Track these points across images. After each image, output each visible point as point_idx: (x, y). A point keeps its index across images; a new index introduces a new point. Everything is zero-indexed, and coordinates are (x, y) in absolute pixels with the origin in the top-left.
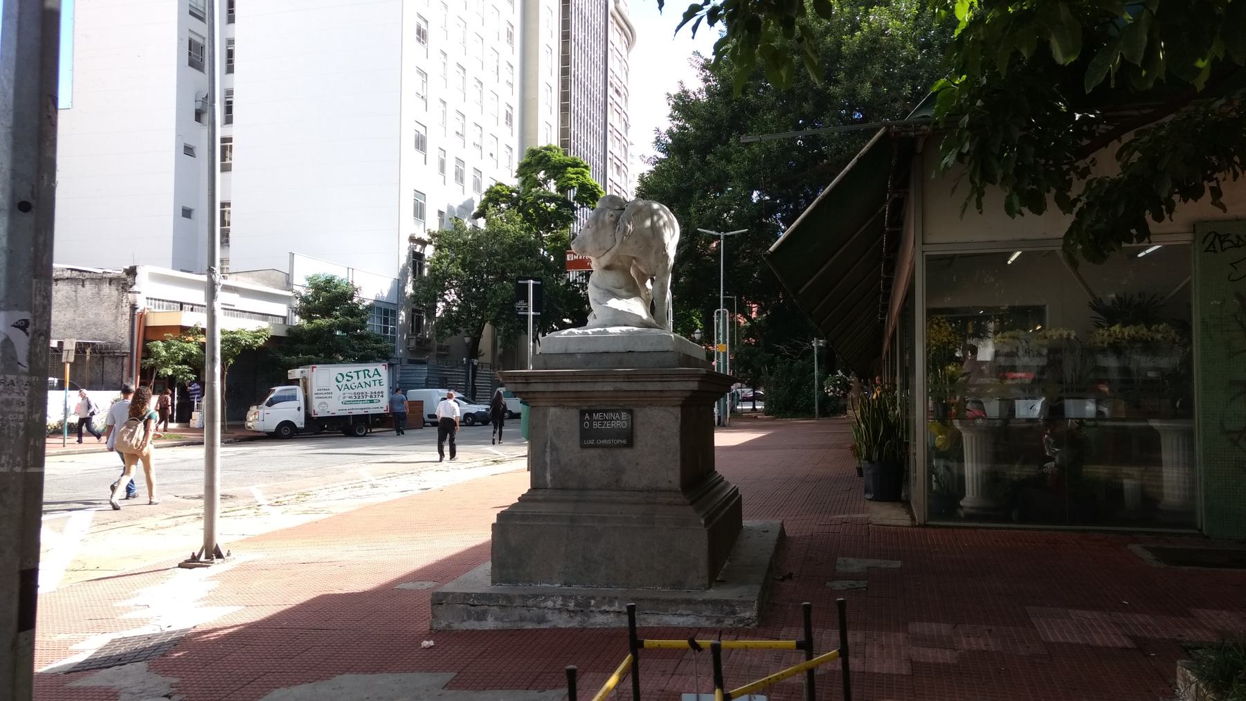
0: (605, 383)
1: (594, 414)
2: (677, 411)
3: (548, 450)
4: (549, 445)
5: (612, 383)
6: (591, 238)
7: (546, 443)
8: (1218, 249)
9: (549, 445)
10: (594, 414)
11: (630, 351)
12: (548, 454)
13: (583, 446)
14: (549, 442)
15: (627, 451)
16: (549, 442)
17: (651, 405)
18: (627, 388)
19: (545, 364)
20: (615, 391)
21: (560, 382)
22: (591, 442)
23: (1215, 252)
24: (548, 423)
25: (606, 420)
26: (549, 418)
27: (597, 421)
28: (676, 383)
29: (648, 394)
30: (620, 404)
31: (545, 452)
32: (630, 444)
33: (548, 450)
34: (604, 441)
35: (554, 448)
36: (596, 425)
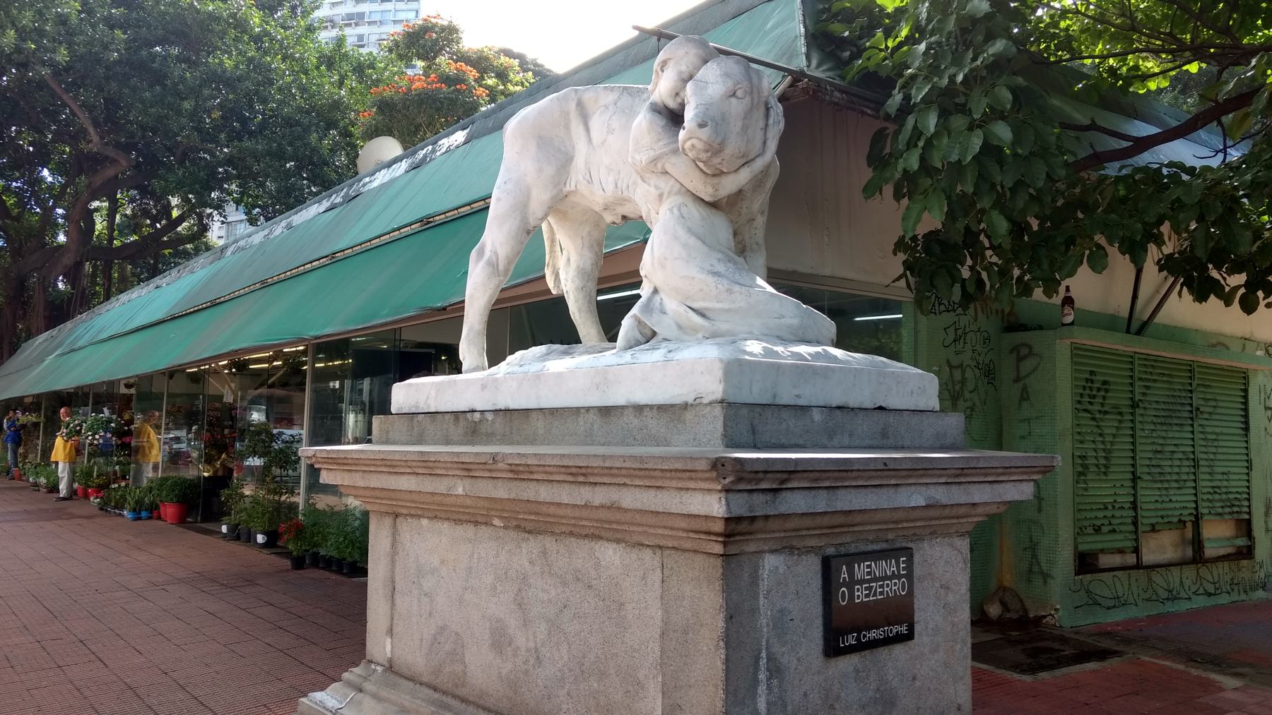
0: (913, 488)
1: (856, 565)
2: (964, 544)
3: (762, 676)
4: (763, 662)
5: (923, 489)
6: (739, 124)
7: (758, 658)
8: (937, 312)
9: (763, 662)
10: (856, 565)
11: (881, 408)
12: (762, 689)
13: (833, 649)
14: (764, 655)
15: (898, 650)
16: (764, 655)
17: (933, 534)
18: (945, 501)
19: (754, 433)
20: (927, 507)
21: (837, 487)
22: (851, 640)
23: (935, 313)
24: (762, 601)
25: (875, 579)
26: (764, 585)
27: (861, 582)
28: (1008, 486)
29: (947, 512)
30: (890, 536)
31: (756, 682)
32: (909, 636)
33: (762, 676)
34: (873, 634)
35: (776, 670)
36: (860, 594)
